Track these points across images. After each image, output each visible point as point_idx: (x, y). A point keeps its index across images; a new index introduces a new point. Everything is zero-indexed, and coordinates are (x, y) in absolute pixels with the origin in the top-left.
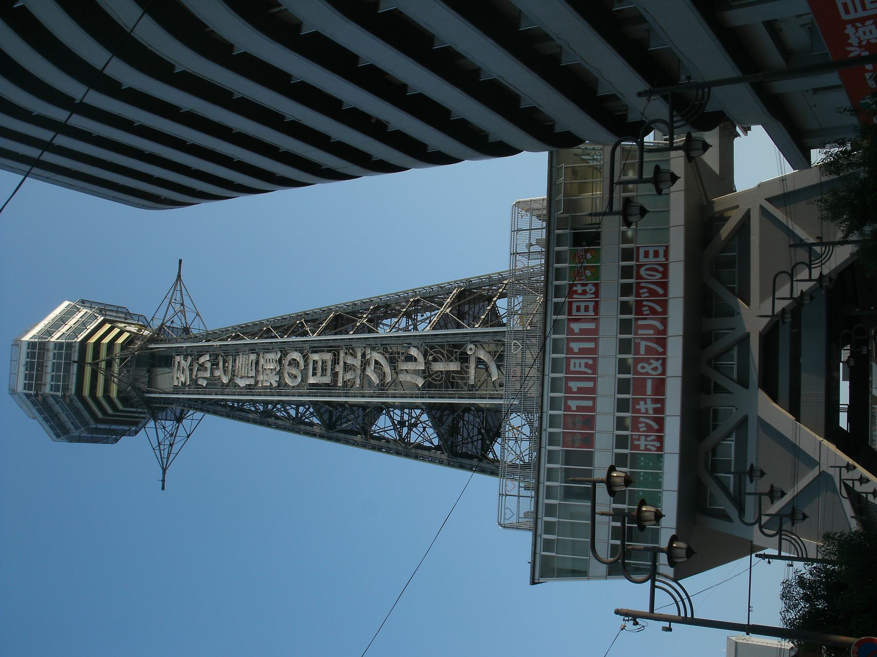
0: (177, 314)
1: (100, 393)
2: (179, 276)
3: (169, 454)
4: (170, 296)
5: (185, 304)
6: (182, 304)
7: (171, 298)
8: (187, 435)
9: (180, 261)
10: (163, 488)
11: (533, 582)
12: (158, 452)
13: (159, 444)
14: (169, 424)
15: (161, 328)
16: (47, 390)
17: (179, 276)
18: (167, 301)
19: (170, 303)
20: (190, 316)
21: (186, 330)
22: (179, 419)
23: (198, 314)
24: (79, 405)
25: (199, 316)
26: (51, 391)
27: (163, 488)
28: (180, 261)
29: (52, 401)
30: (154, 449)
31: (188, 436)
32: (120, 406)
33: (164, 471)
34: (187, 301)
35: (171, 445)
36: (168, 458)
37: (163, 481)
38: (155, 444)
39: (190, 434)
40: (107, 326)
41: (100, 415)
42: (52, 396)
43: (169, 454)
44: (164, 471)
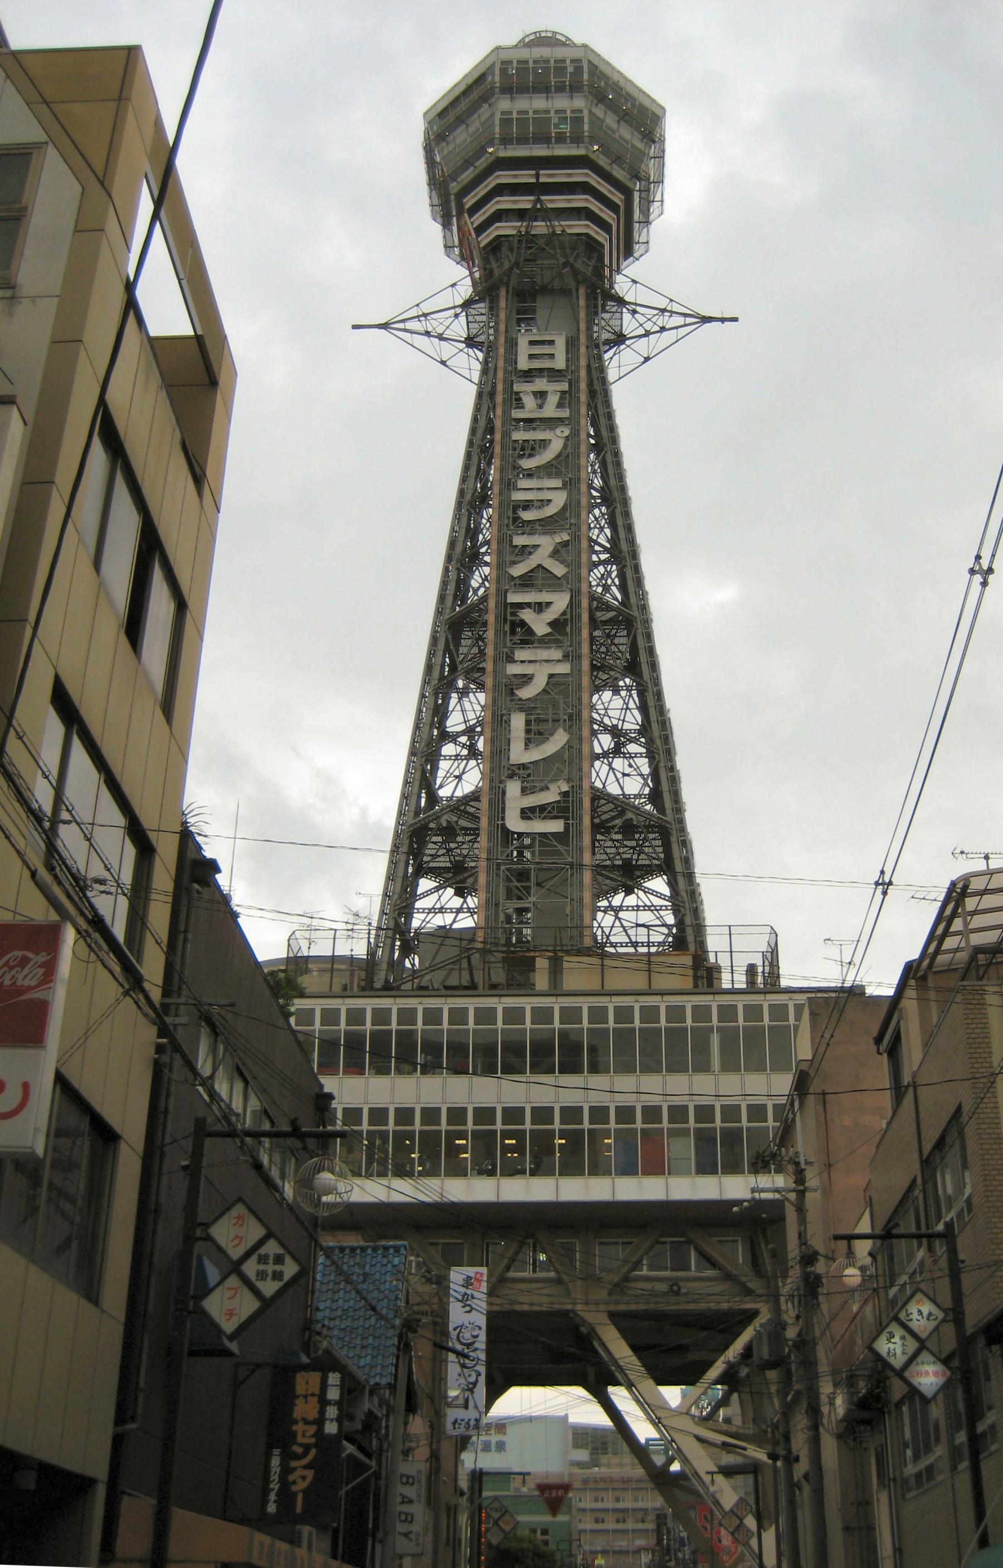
0: (641, 325)
1: (505, 202)
2: (706, 320)
3: (412, 332)
4: (676, 308)
5: (665, 333)
6: (663, 329)
7: (672, 312)
8: (444, 359)
12: (414, 313)
13: (425, 315)
14: (459, 328)
15: (621, 302)
16: (504, 104)
17: (706, 320)
18: (662, 303)
19: (663, 311)
20: (642, 346)
22: (470, 342)
23: (647, 359)
24: (482, 163)
25: (644, 363)
26: (503, 113)
29: (484, 111)
30: (417, 305)
31: (443, 363)
32: (485, 239)
33: (385, 326)
34: (669, 336)
35: (427, 333)
36: (405, 330)
38: (426, 308)
39: (447, 366)
40: (617, 198)
42: (493, 115)
43: (412, 332)
44: (385, 326)
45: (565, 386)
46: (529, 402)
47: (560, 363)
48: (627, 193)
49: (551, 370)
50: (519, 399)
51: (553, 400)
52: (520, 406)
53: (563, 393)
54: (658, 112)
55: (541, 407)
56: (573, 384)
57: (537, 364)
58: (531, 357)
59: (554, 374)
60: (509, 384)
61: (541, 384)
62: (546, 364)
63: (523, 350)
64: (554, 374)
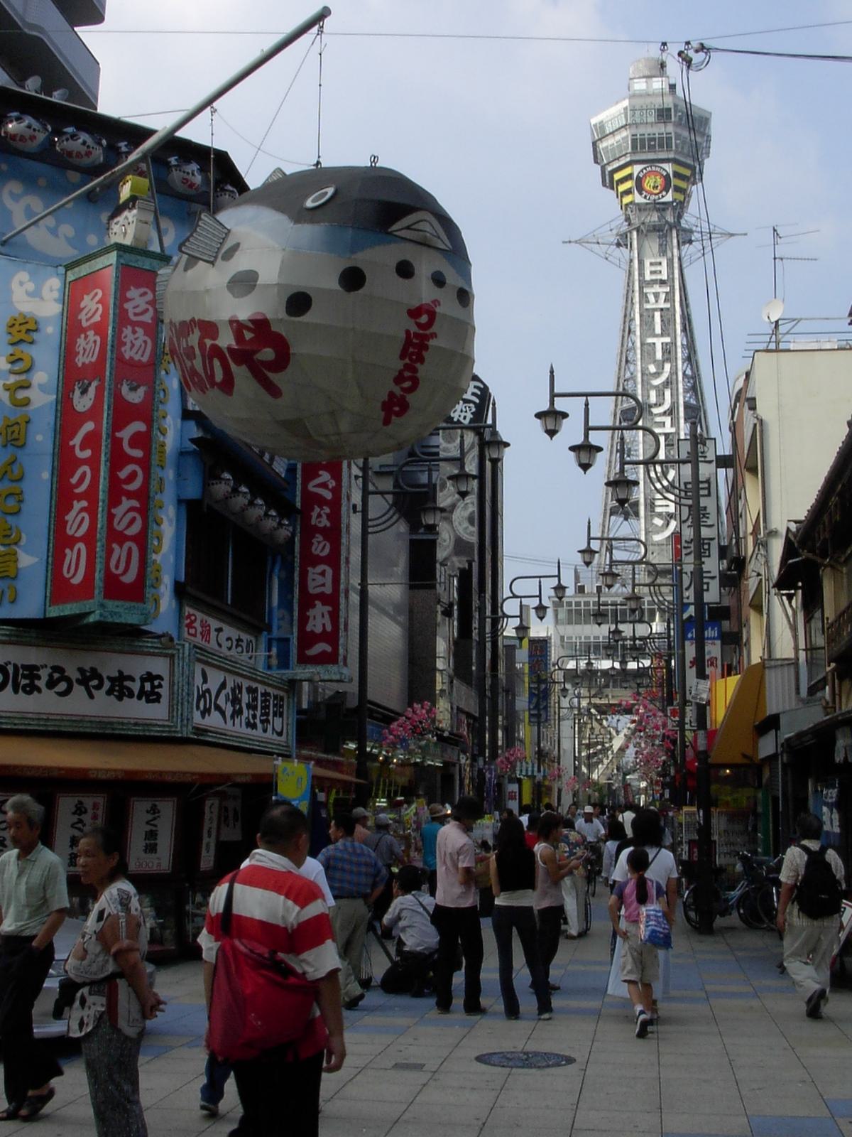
2: (732, 235)
9: (746, 234)
10: (564, 242)
11: (549, 598)
14: (614, 239)
17: (732, 235)
21: (690, 242)
24: (622, 162)
27: (564, 242)
28: (746, 234)
32: (627, 200)
33: (576, 242)
37: (570, 242)
40: (687, 172)
41: (617, 176)
44: (576, 242)
45: (668, 289)
46: (652, 298)
47: (665, 277)
48: (692, 168)
49: (661, 280)
50: (647, 297)
51: (663, 297)
52: (648, 302)
53: (667, 293)
54: (708, 116)
55: (657, 301)
56: (673, 288)
57: (654, 277)
58: (652, 273)
59: (662, 282)
60: (641, 288)
61: (657, 288)
62: (659, 277)
63: (648, 269)
64: (662, 282)
